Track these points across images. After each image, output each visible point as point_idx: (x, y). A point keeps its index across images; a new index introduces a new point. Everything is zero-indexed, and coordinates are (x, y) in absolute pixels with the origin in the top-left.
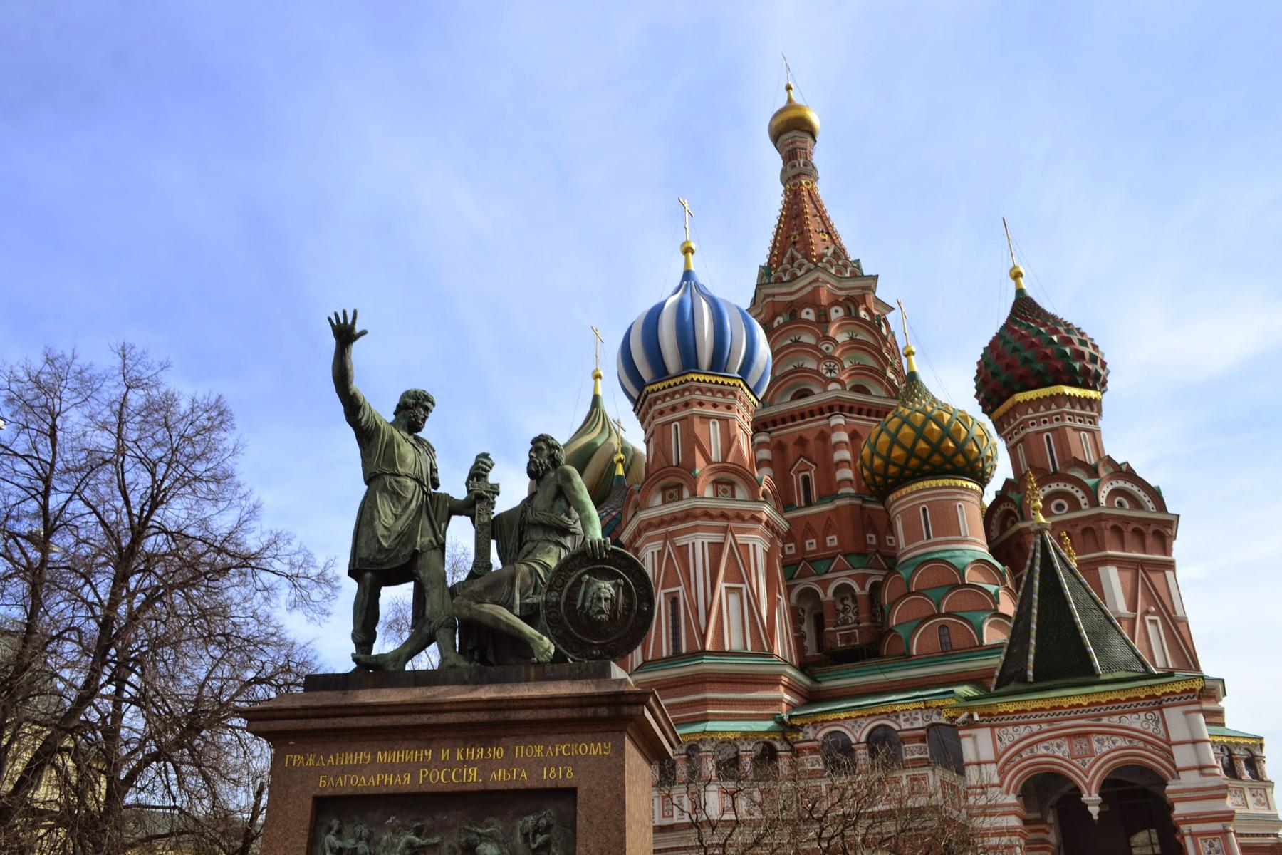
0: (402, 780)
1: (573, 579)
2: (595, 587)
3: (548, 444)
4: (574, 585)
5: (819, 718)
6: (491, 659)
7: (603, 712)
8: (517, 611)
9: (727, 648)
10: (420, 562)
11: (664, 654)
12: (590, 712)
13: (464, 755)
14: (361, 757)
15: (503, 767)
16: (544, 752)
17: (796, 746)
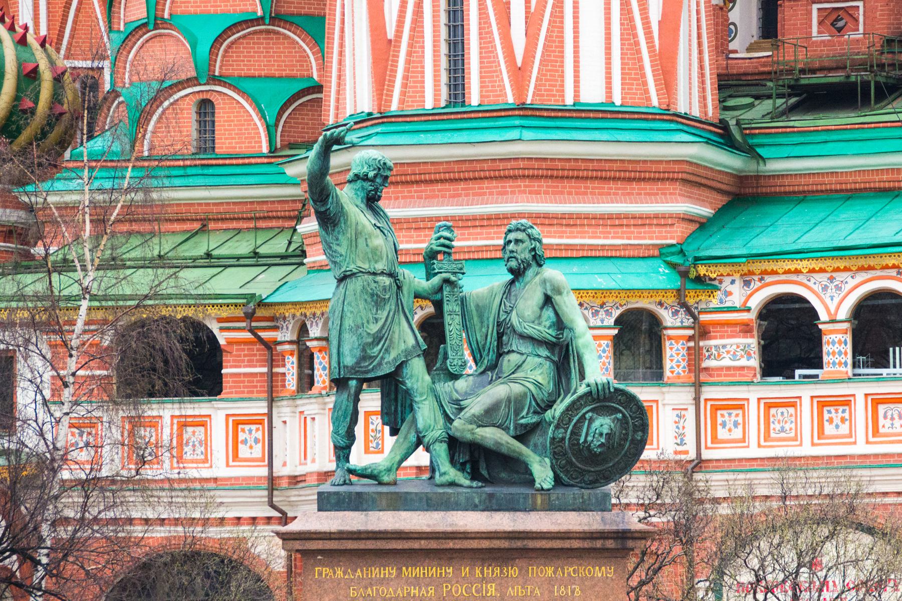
0: (427, 592)
1: (577, 417)
2: (597, 424)
3: (529, 235)
4: (578, 421)
5: (757, 267)
6: (484, 472)
7: (610, 544)
8: (512, 432)
9: (569, 101)
10: (406, 371)
11: (429, 104)
12: (599, 544)
13: (482, 573)
14: (390, 571)
15: (518, 584)
16: (555, 572)
17: (703, 318)
